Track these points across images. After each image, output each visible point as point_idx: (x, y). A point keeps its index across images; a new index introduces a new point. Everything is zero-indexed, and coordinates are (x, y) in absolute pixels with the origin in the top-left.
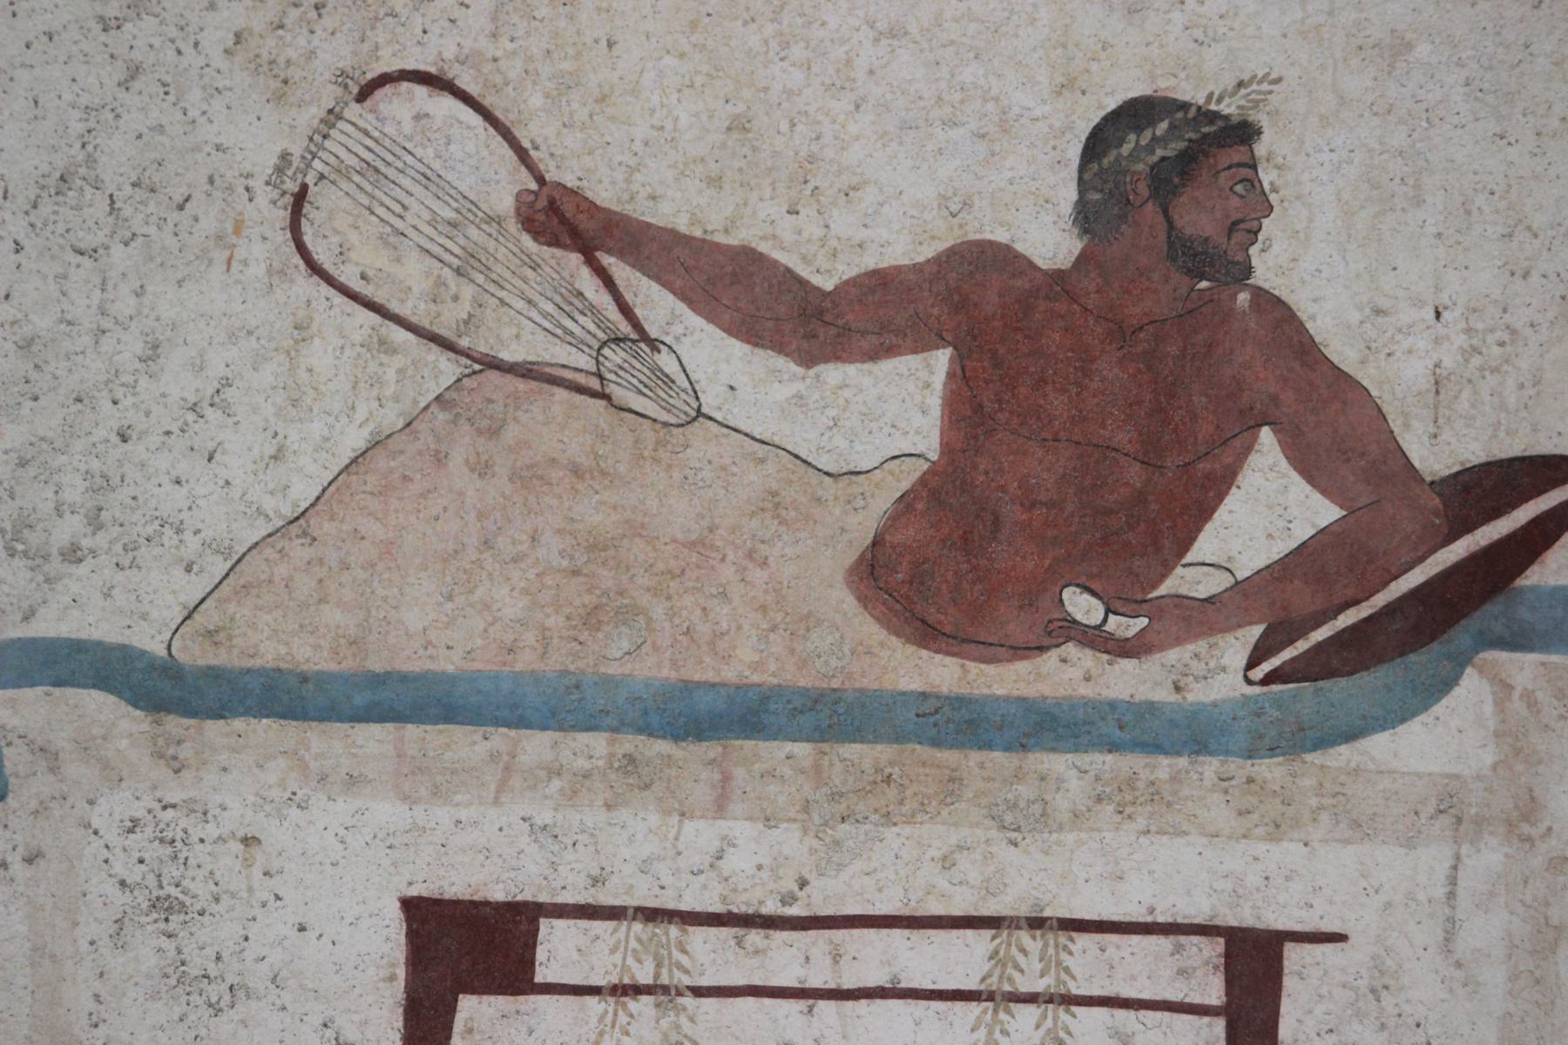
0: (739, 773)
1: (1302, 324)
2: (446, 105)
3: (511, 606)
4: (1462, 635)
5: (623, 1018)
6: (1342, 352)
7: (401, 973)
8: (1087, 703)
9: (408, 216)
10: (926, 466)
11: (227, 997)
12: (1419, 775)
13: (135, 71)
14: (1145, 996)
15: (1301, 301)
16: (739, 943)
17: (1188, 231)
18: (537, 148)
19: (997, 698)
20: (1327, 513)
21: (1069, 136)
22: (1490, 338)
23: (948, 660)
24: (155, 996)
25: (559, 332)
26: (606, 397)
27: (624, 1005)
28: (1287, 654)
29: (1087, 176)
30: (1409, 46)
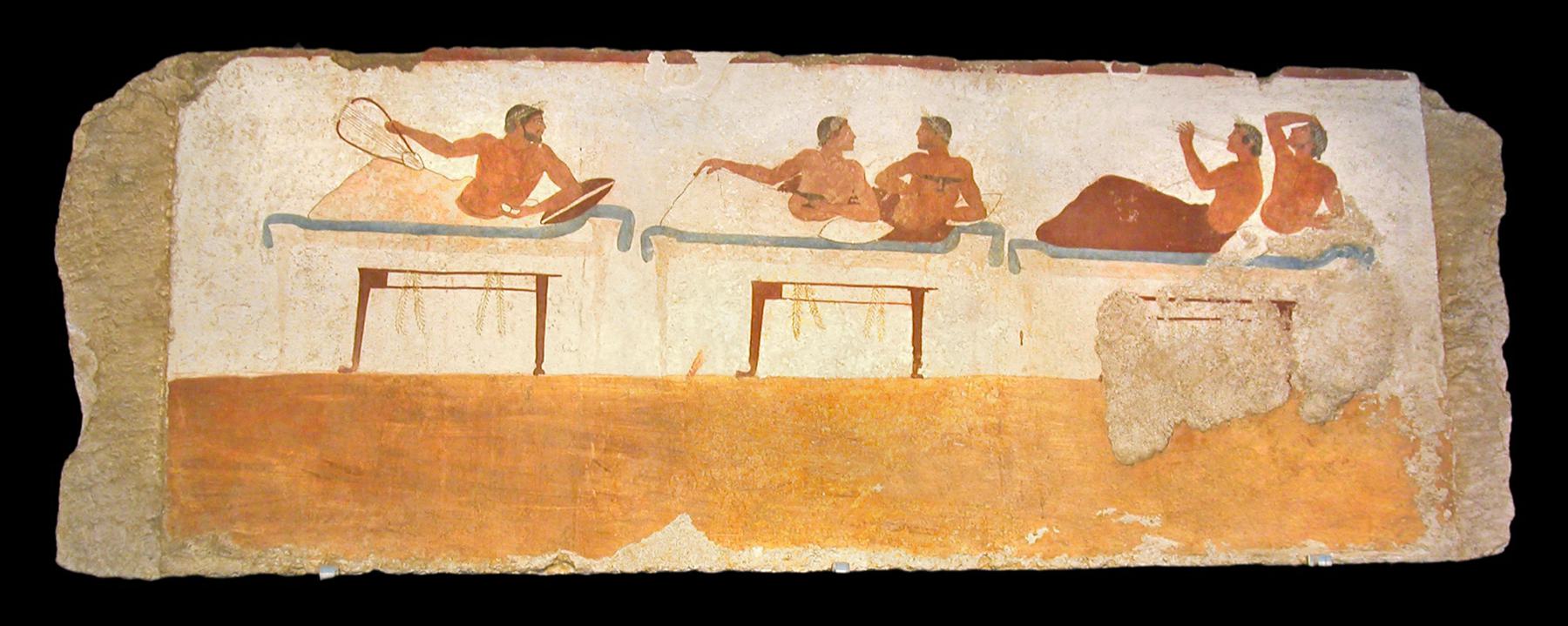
3: (382, 207)
20: (558, 189)
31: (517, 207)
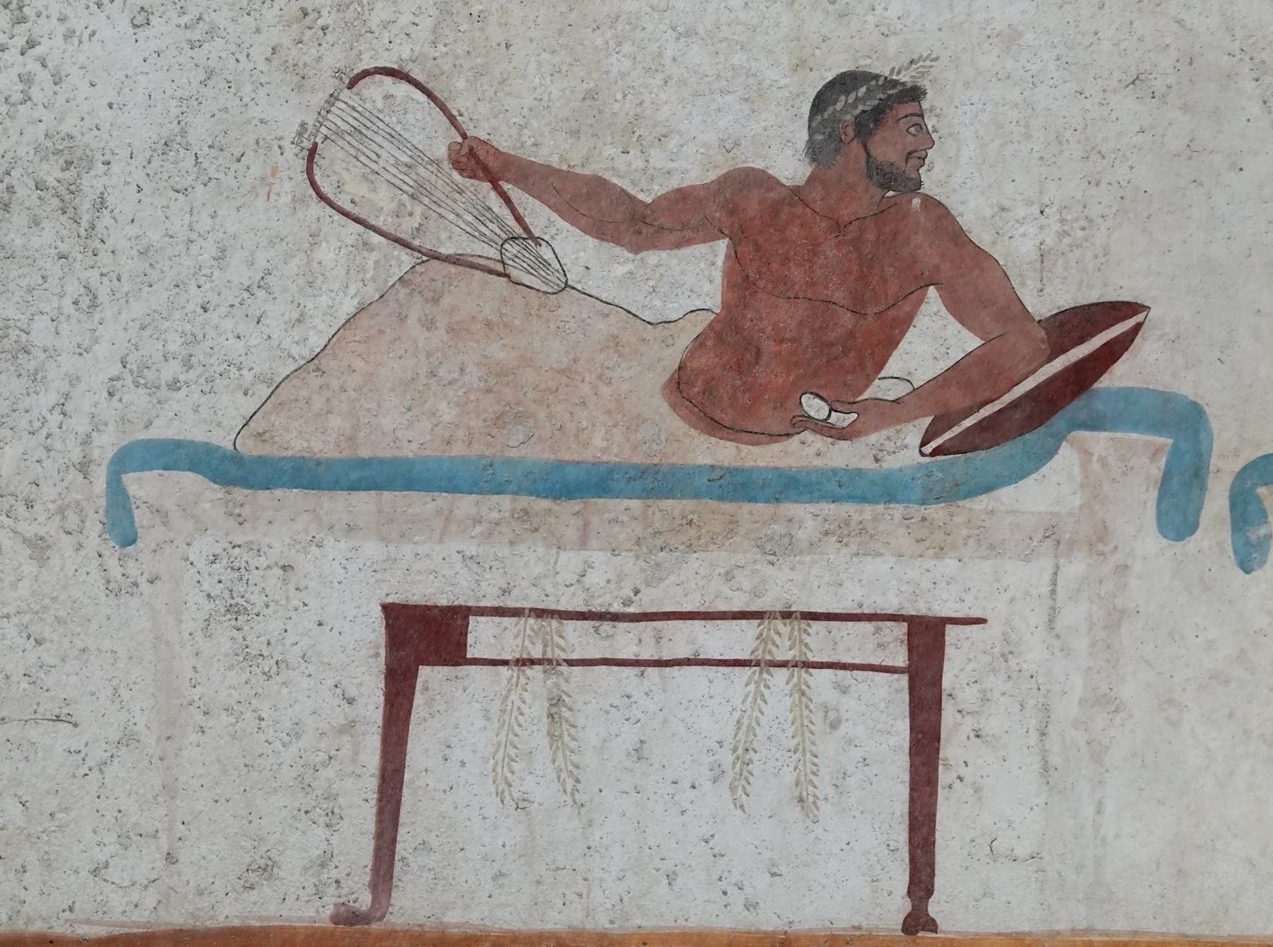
0: (595, 520)
1: (954, 218)
2: (403, 89)
3: (448, 413)
4: (1059, 421)
5: (523, 680)
6: (981, 237)
7: (383, 652)
8: (817, 470)
9: (381, 162)
10: (713, 317)
11: (275, 668)
12: (1032, 514)
13: (210, 74)
14: (857, 661)
15: (953, 204)
16: (597, 630)
17: (880, 159)
18: (461, 115)
19: (760, 468)
21: (802, 98)
22: (1075, 225)
23: (728, 443)
24: (231, 668)
25: (476, 234)
26: (507, 276)
27: (524, 672)
28: (947, 436)
29: (814, 124)
30: (1020, 34)
31: (850, 406)
